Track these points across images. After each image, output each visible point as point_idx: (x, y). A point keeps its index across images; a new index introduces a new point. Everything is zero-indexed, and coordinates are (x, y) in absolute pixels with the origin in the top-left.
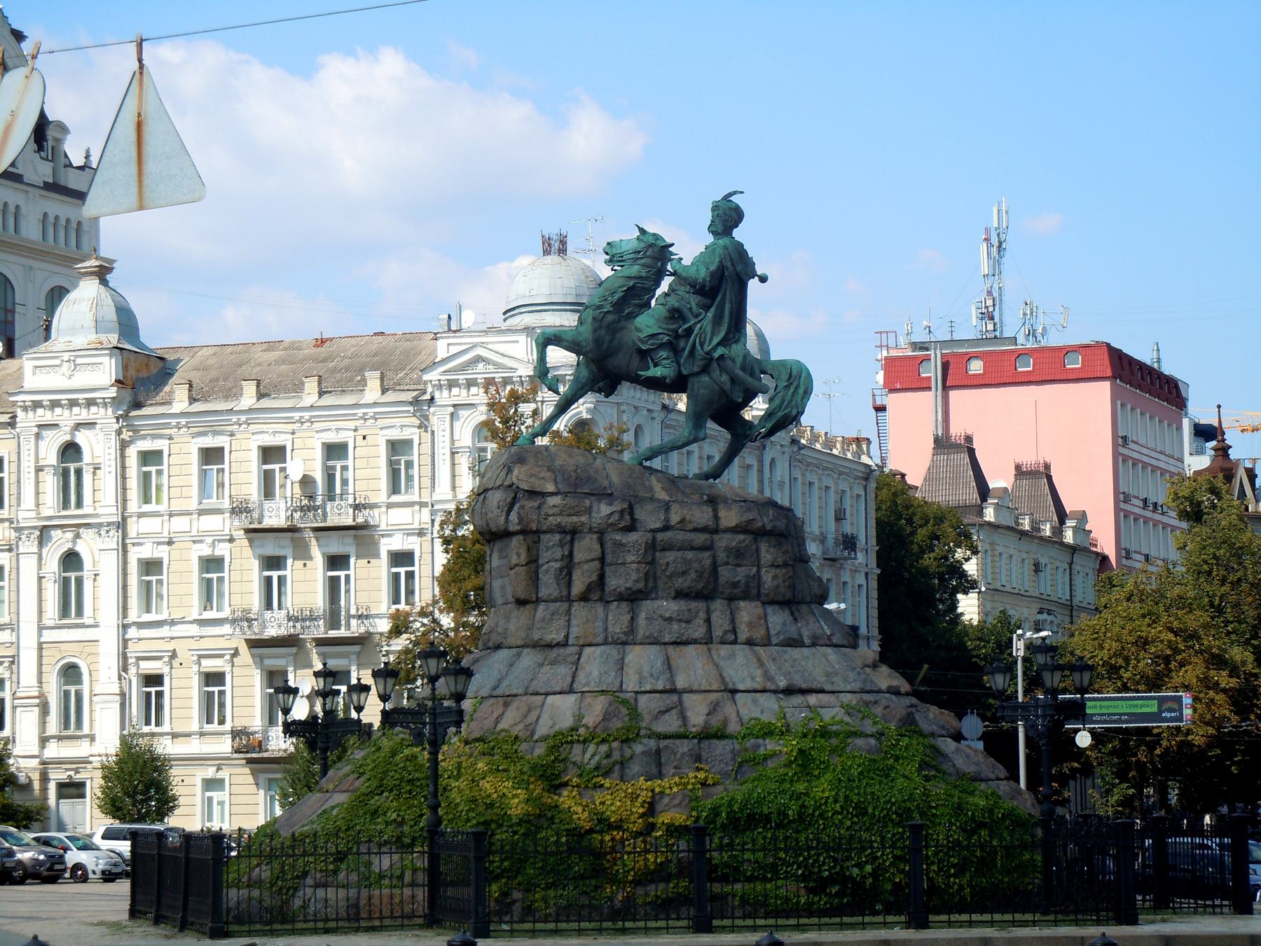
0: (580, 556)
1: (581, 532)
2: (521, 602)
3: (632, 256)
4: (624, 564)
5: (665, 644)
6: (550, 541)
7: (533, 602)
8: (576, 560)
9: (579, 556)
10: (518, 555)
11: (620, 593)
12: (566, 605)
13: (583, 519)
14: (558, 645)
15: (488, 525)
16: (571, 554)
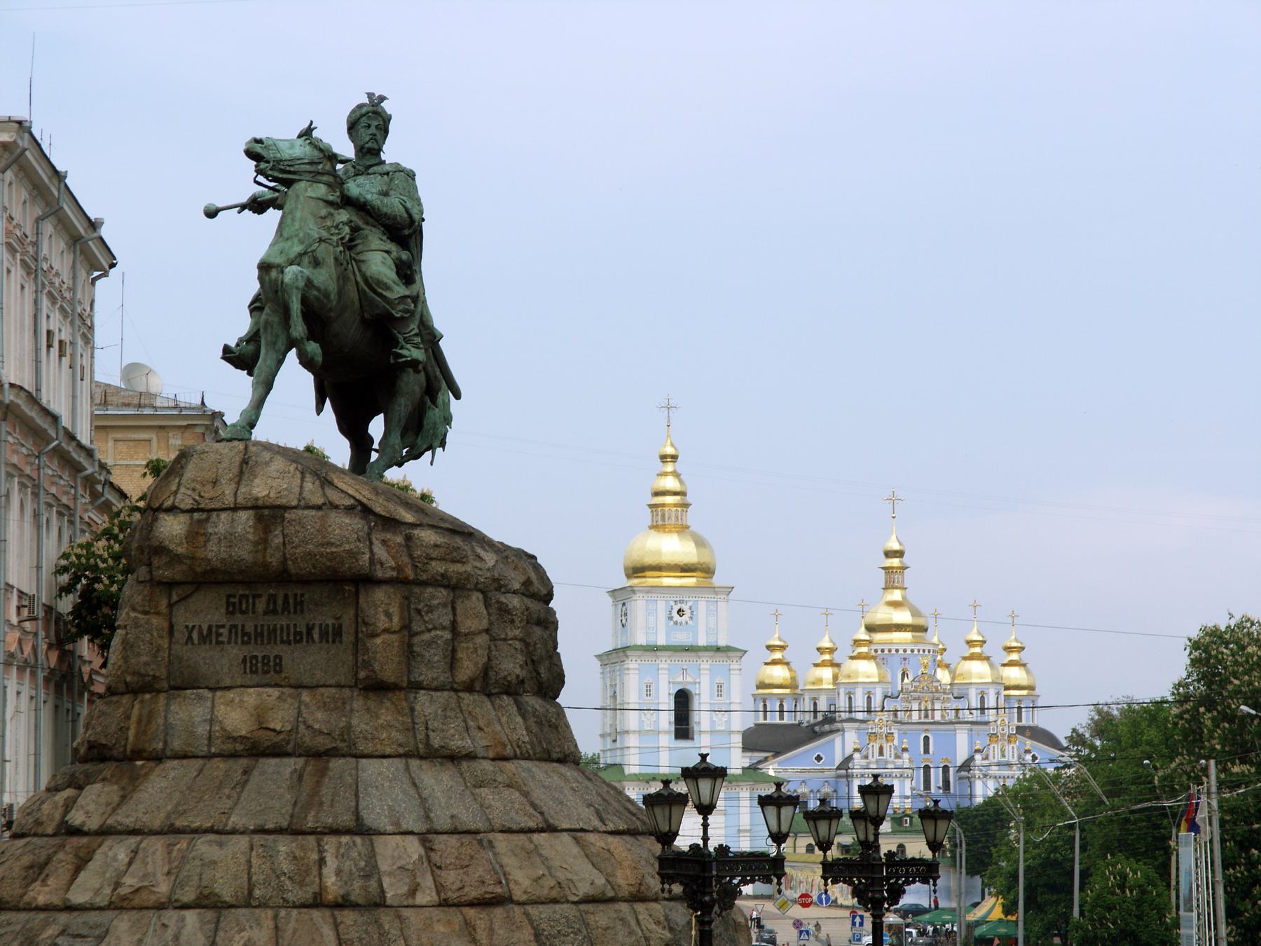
0: (469, 623)
1: (463, 588)
2: (377, 688)
3: (308, 167)
4: (505, 640)
5: (553, 761)
6: (433, 597)
7: (400, 688)
8: (463, 629)
9: (467, 625)
10: (388, 615)
11: (510, 682)
12: (452, 694)
13: (468, 568)
14: (471, 757)
15: (285, 559)
16: (454, 623)
